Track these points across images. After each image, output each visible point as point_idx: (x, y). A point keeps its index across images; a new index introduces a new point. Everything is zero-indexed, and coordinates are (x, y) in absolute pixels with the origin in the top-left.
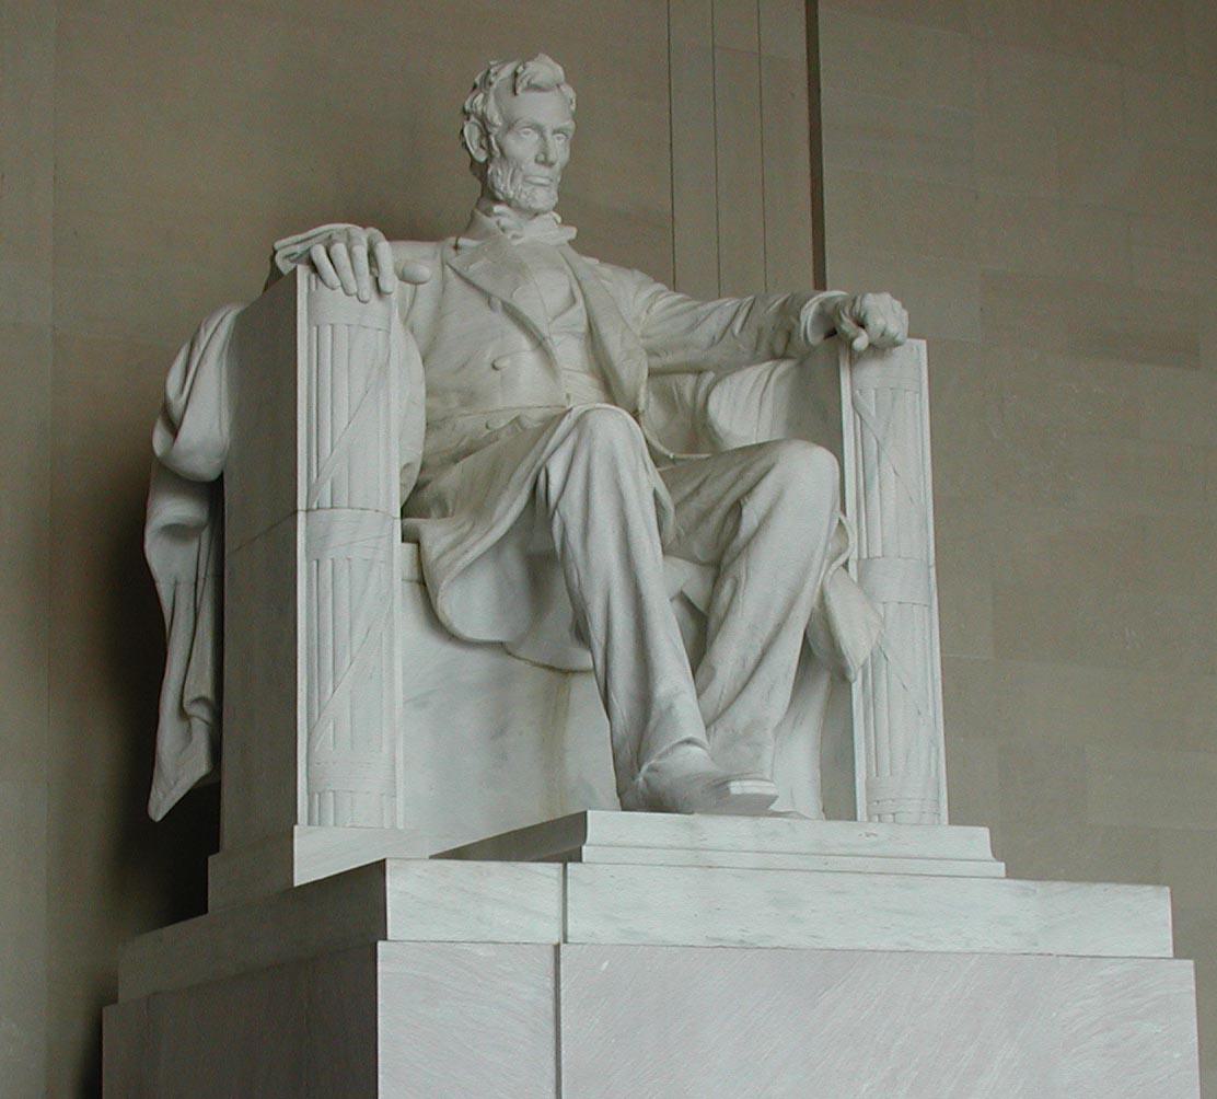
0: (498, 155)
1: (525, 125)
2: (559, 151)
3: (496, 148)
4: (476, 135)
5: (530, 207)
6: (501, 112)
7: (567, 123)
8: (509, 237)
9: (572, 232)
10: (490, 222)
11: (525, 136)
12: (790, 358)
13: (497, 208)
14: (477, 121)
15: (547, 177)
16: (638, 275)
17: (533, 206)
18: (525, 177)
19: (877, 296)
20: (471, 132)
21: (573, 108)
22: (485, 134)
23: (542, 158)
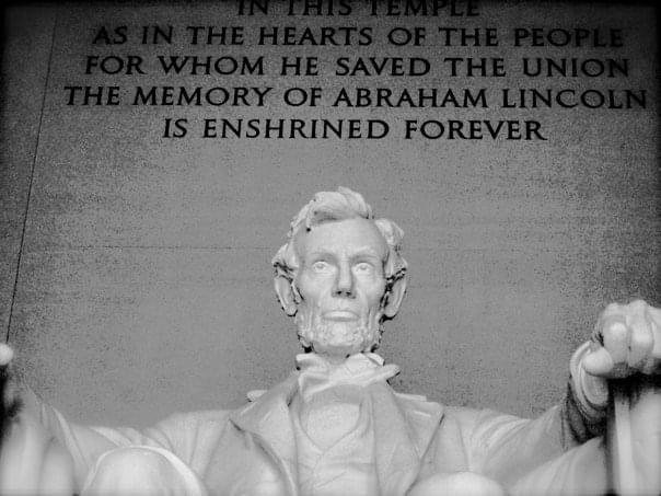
0: (299, 300)
1: (316, 257)
2: (369, 284)
3: (297, 293)
4: (287, 291)
5: (329, 345)
6: (297, 254)
7: (365, 248)
8: (301, 381)
9: (390, 370)
10: (297, 372)
11: (317, 270)
12: (594, 436)
13: (302, 357)
14: (283, 273)
15: (346, 310)
16: (485, 412)
17: (332, 343)
18: (323, 314)
19: (626, 307)
20: (280, 285)
21: (390, 241)
22: (291, 281)
23: (335, 290)
